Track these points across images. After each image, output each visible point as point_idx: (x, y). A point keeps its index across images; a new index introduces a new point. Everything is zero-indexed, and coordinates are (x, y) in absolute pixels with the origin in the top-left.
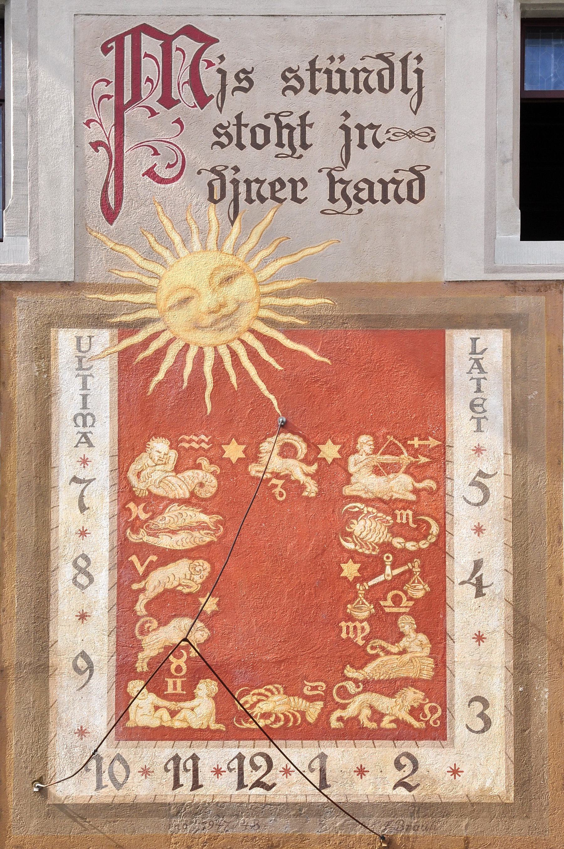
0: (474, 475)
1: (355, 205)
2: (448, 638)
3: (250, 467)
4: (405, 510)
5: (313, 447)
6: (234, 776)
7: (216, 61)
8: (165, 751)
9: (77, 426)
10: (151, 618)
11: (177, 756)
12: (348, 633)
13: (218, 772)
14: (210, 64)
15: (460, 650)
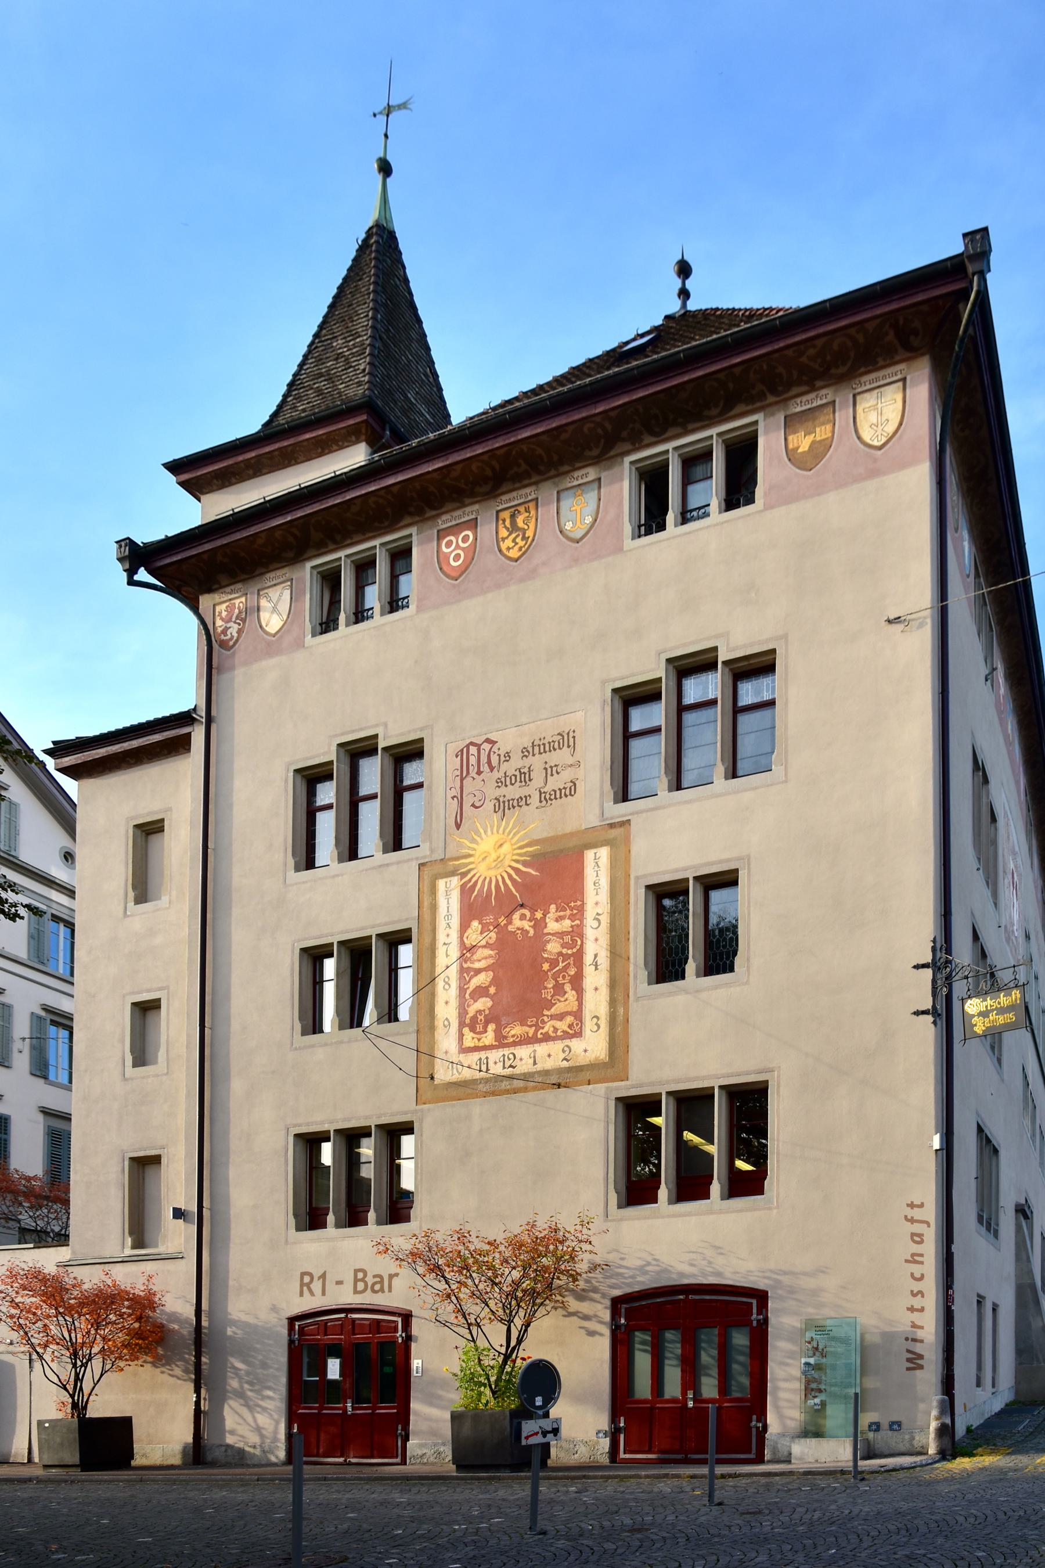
5: (533, 914)
15: (589, 996)
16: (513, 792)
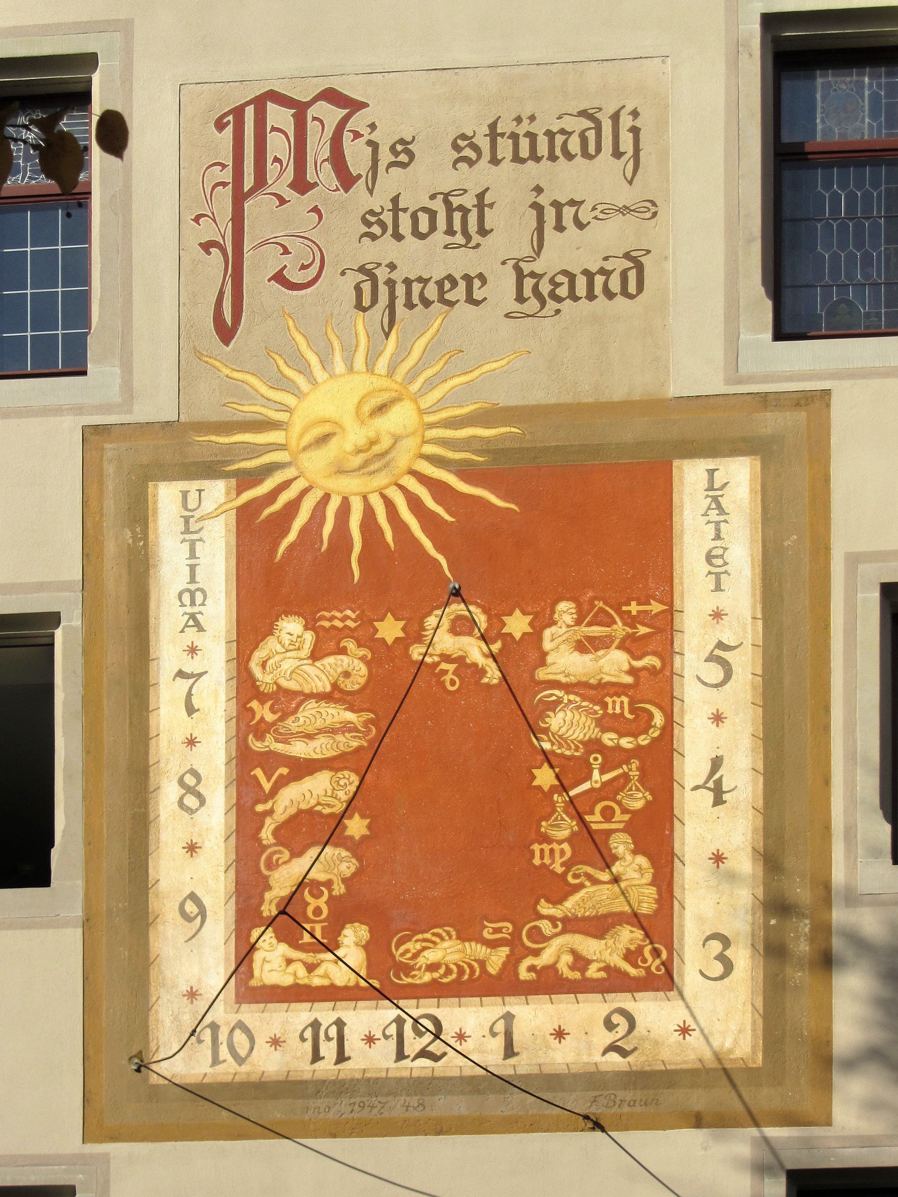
0: (712, 647)
1: (551, 305)
2: (676, 860)
3: (411, 648)
4: (619, 697)
5: (496, 618)
6: (392, 1044)
7: (365, 131)
8: (301, 1015)
9: (183, 605)
10: (281, 848)
11: (316, 1020)
12: (542, 858)
13: (370, 1040)
14: (357, 135)
15: (692, 874)
16: (421, 258)
